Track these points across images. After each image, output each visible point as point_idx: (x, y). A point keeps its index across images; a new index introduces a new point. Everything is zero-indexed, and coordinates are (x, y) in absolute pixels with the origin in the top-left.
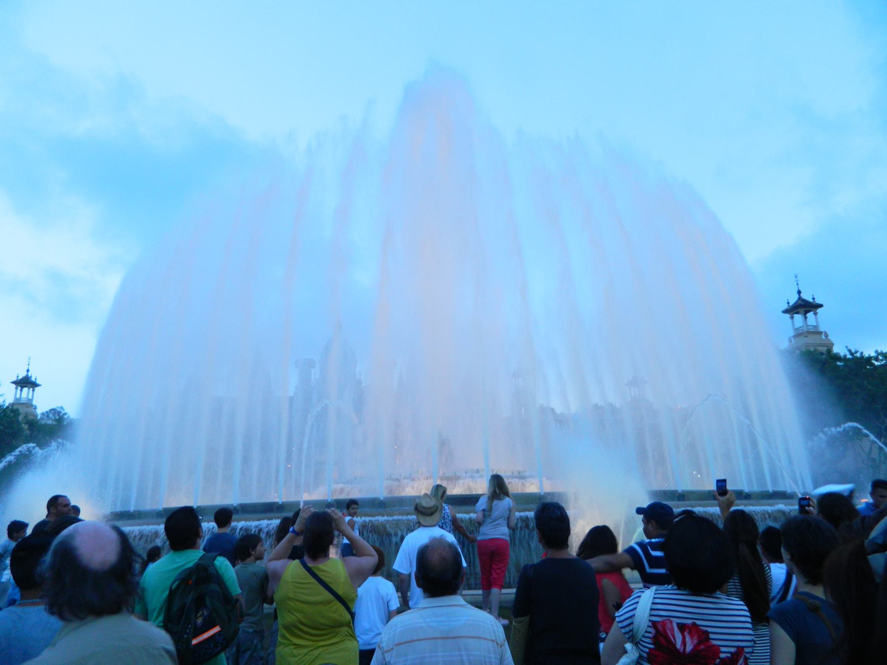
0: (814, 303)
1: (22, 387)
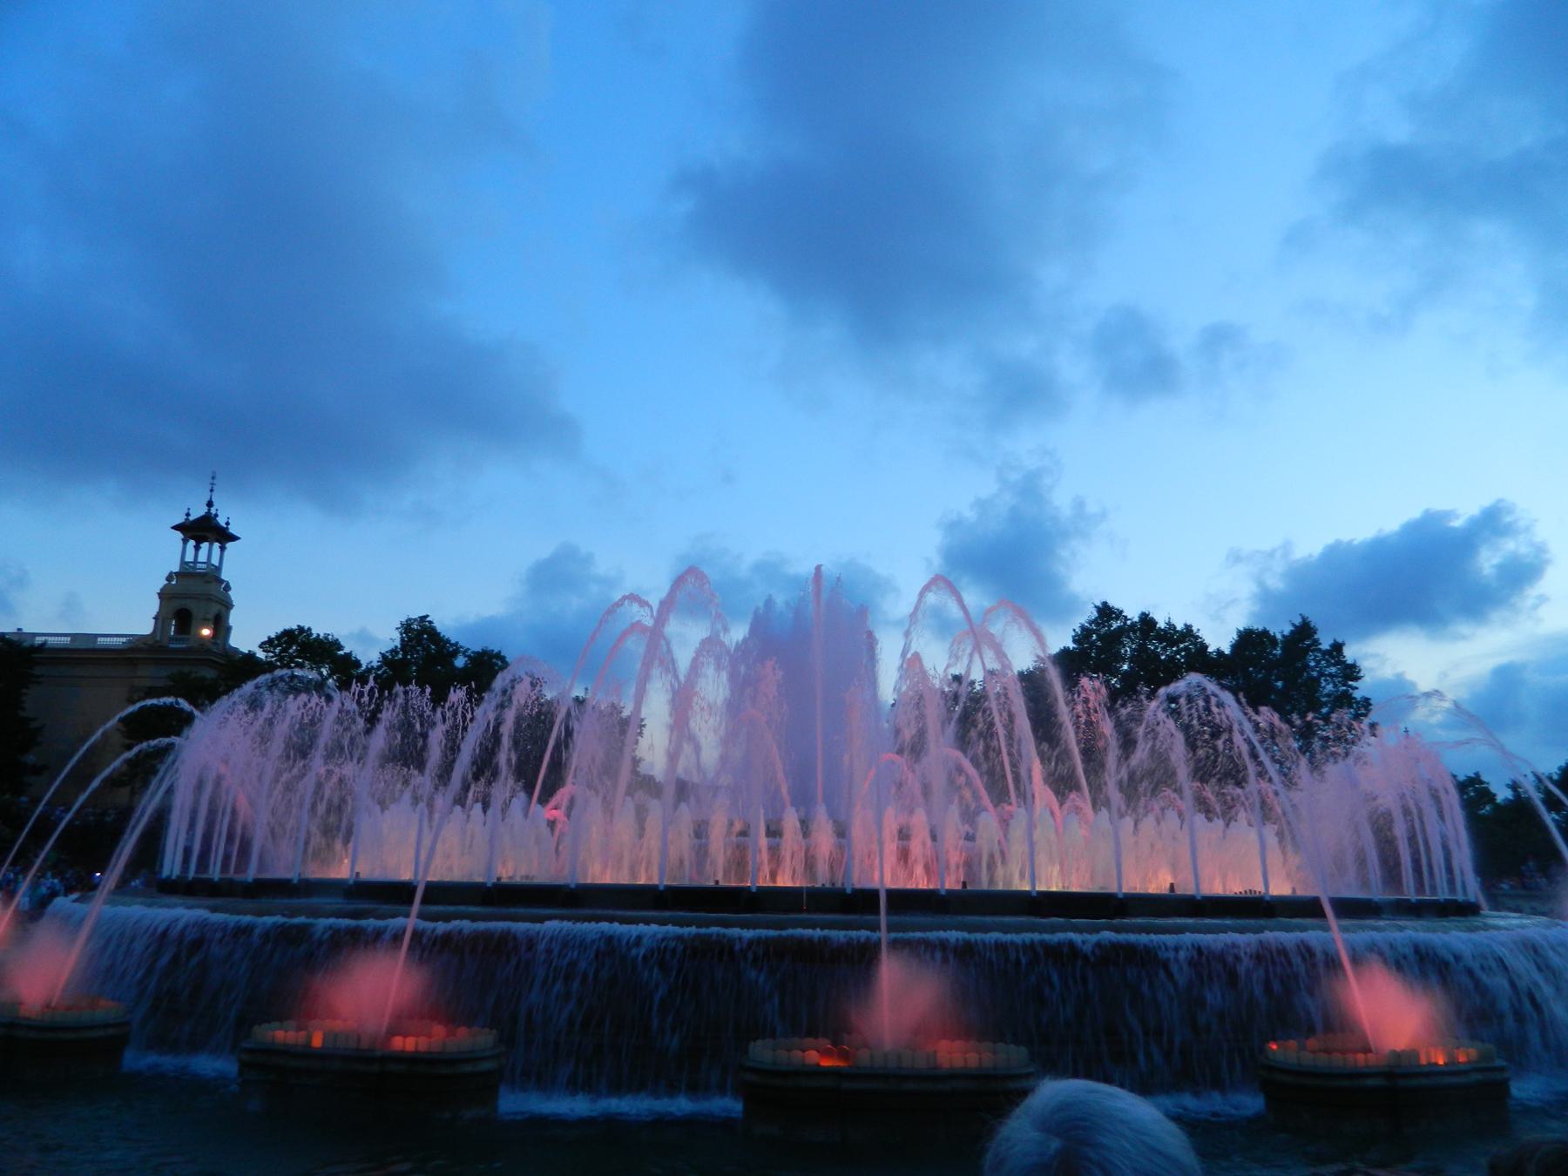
1: (199, 541)
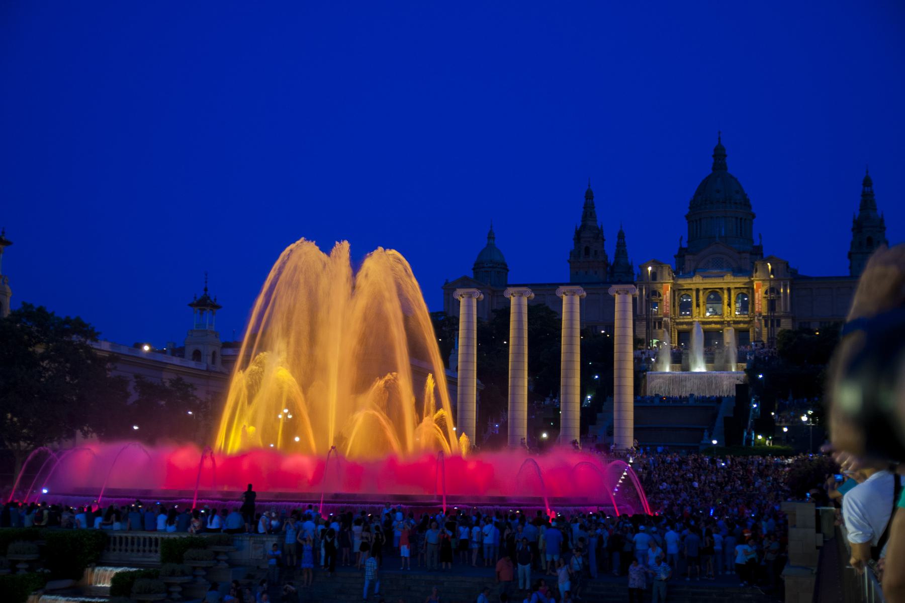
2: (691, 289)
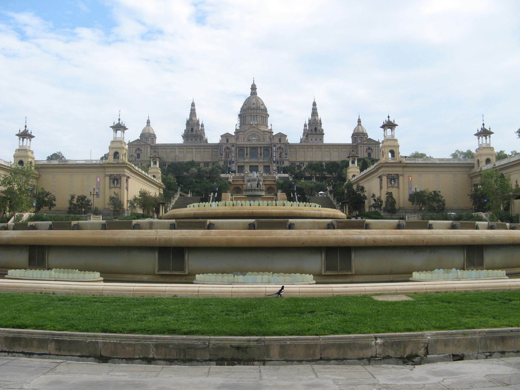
0: (490, 131)
1: (23, 138)
2: (244, 147)
